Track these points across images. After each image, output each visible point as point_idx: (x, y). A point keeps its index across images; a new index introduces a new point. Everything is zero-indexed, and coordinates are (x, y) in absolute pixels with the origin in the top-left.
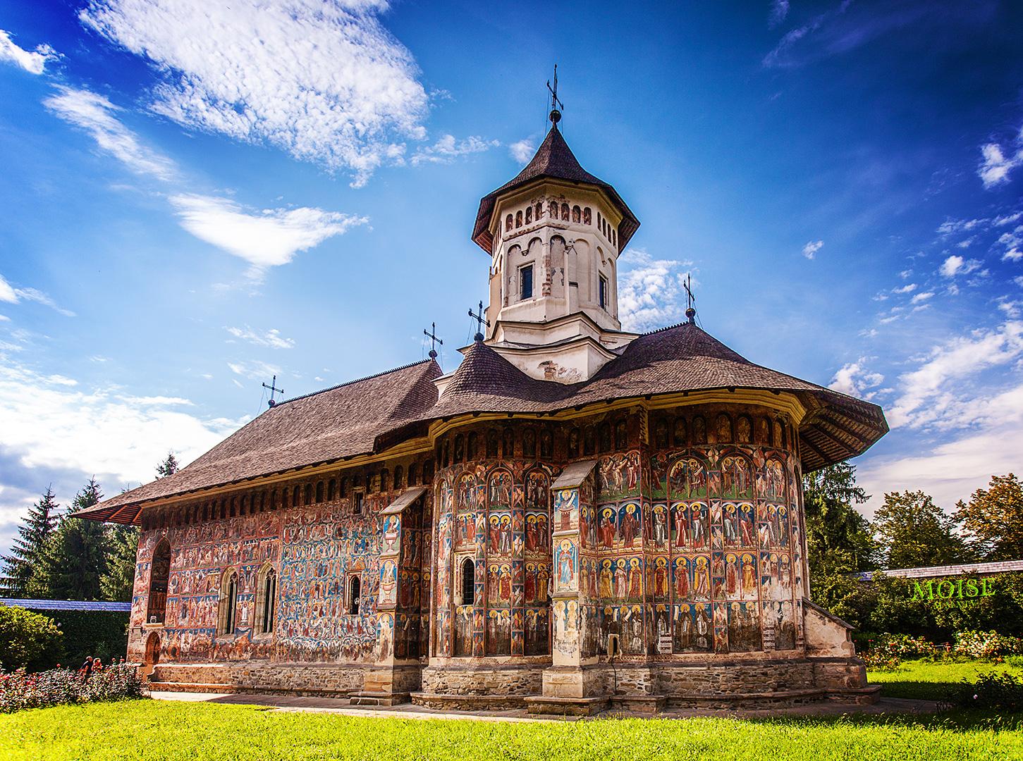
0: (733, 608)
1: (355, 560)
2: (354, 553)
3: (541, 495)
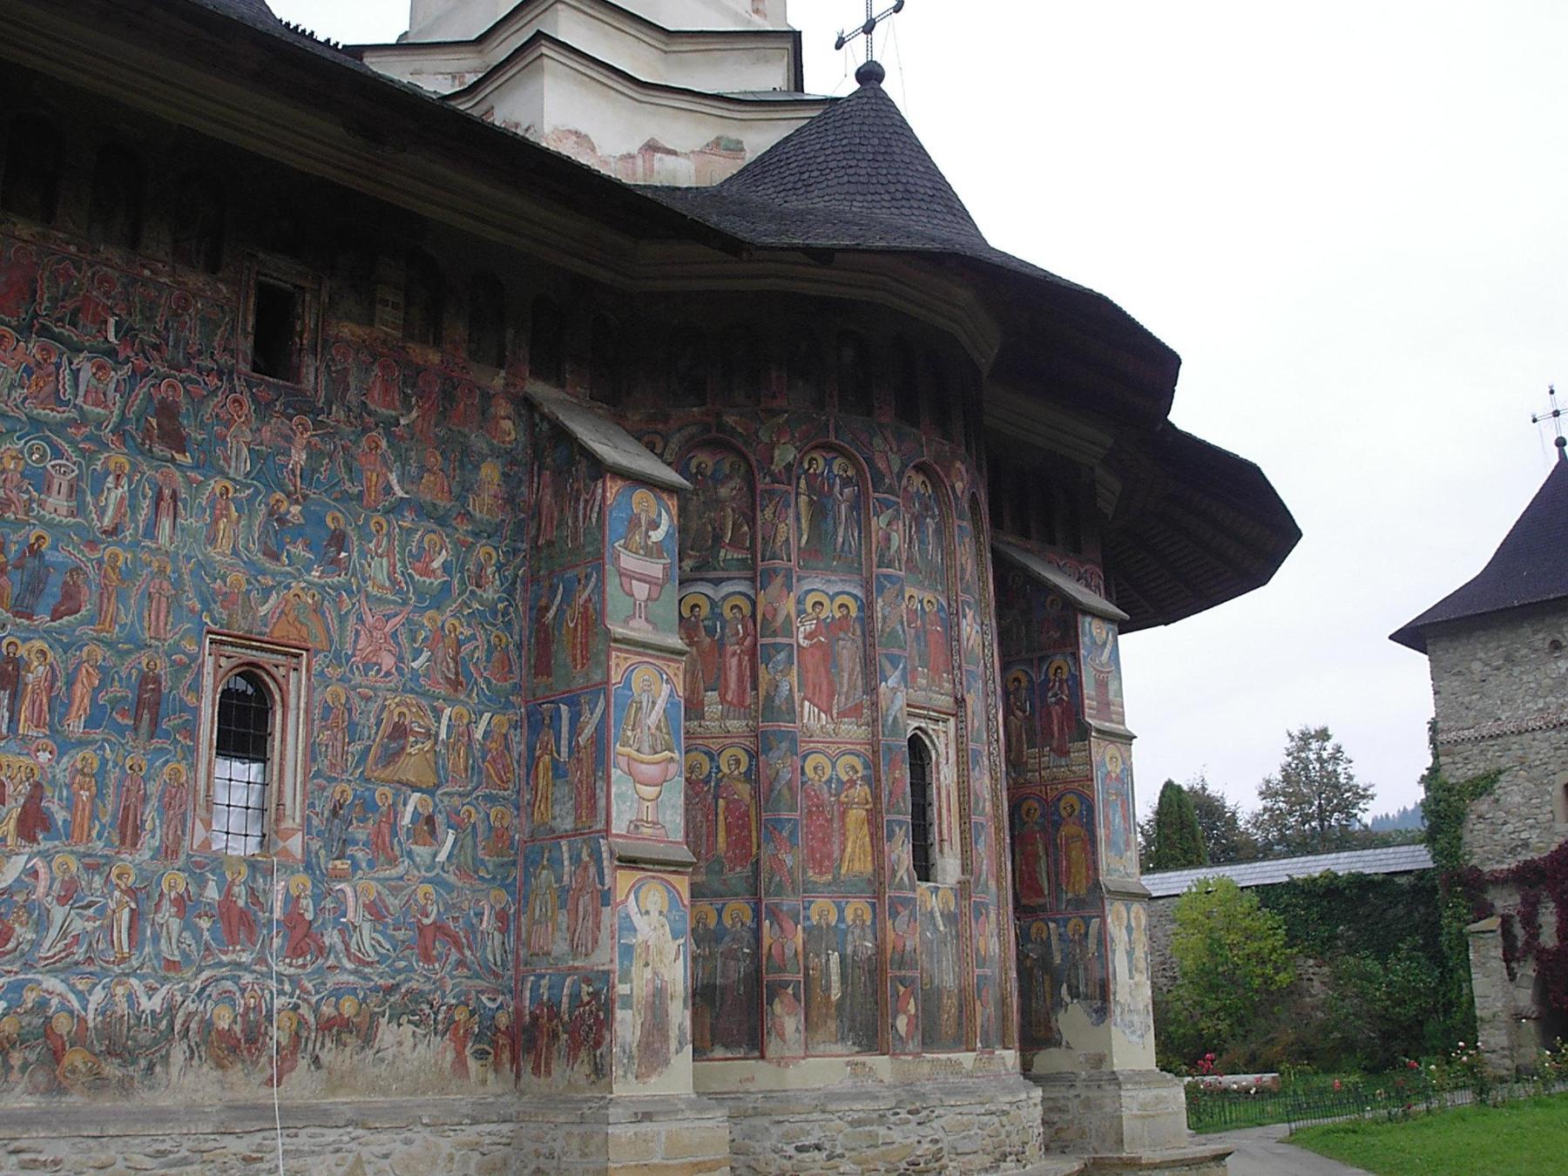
1: (267, 592)
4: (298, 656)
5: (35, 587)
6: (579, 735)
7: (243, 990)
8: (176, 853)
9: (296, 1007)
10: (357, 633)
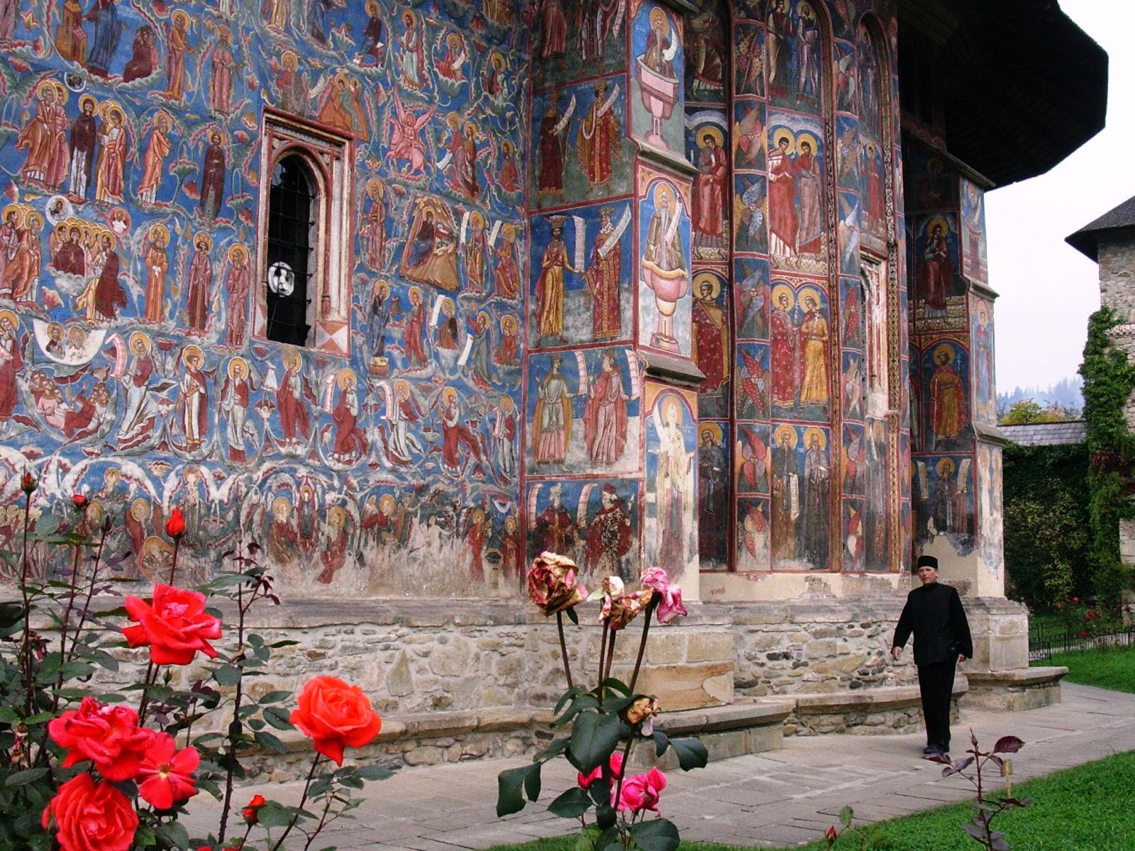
1: (316, 74)
2: (308, 37)
4: (340, 145)
5: (108, 42)
6: (599, 246)
7: (298, 484)
8: (240, 338)
9: (344, 503)
10: (392, 129)
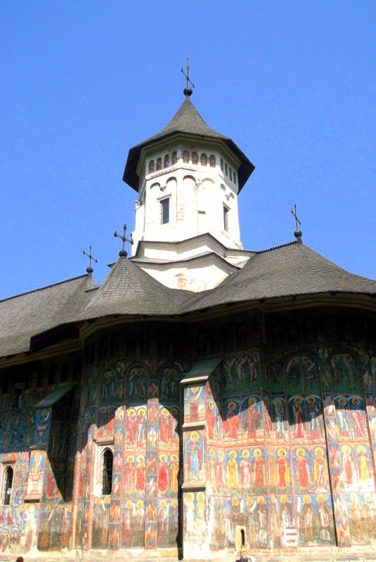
0: (352, 499)
3: (174, 390)
